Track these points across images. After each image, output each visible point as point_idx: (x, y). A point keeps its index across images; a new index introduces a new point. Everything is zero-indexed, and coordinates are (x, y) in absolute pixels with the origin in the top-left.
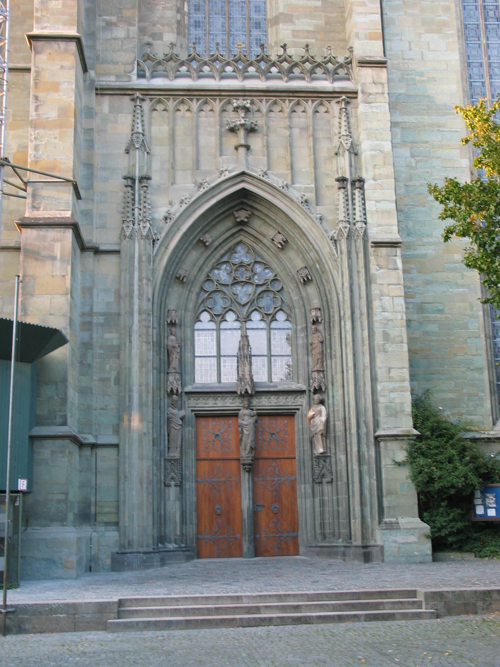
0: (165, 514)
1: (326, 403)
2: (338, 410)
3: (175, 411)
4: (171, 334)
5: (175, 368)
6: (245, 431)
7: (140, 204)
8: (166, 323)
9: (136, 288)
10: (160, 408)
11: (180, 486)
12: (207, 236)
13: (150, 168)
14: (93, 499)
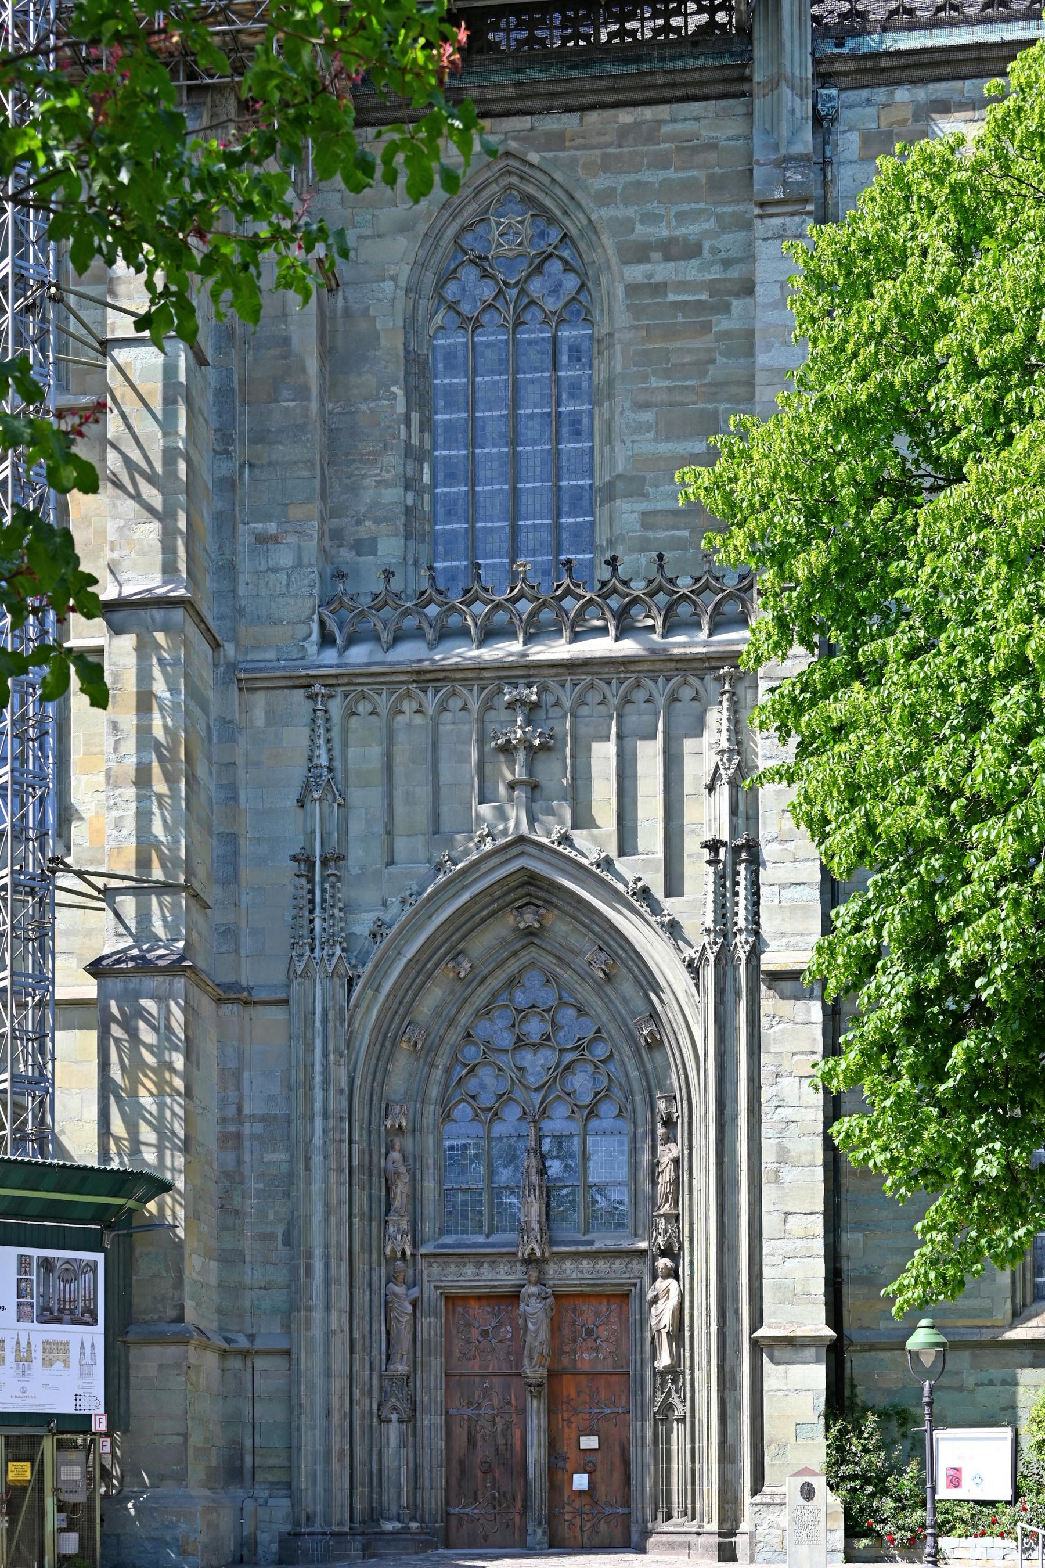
9: (318, 1068)
10: (370, 1285)
11: (411, 1419)
13: (346, 833)
14: (248, 1443)
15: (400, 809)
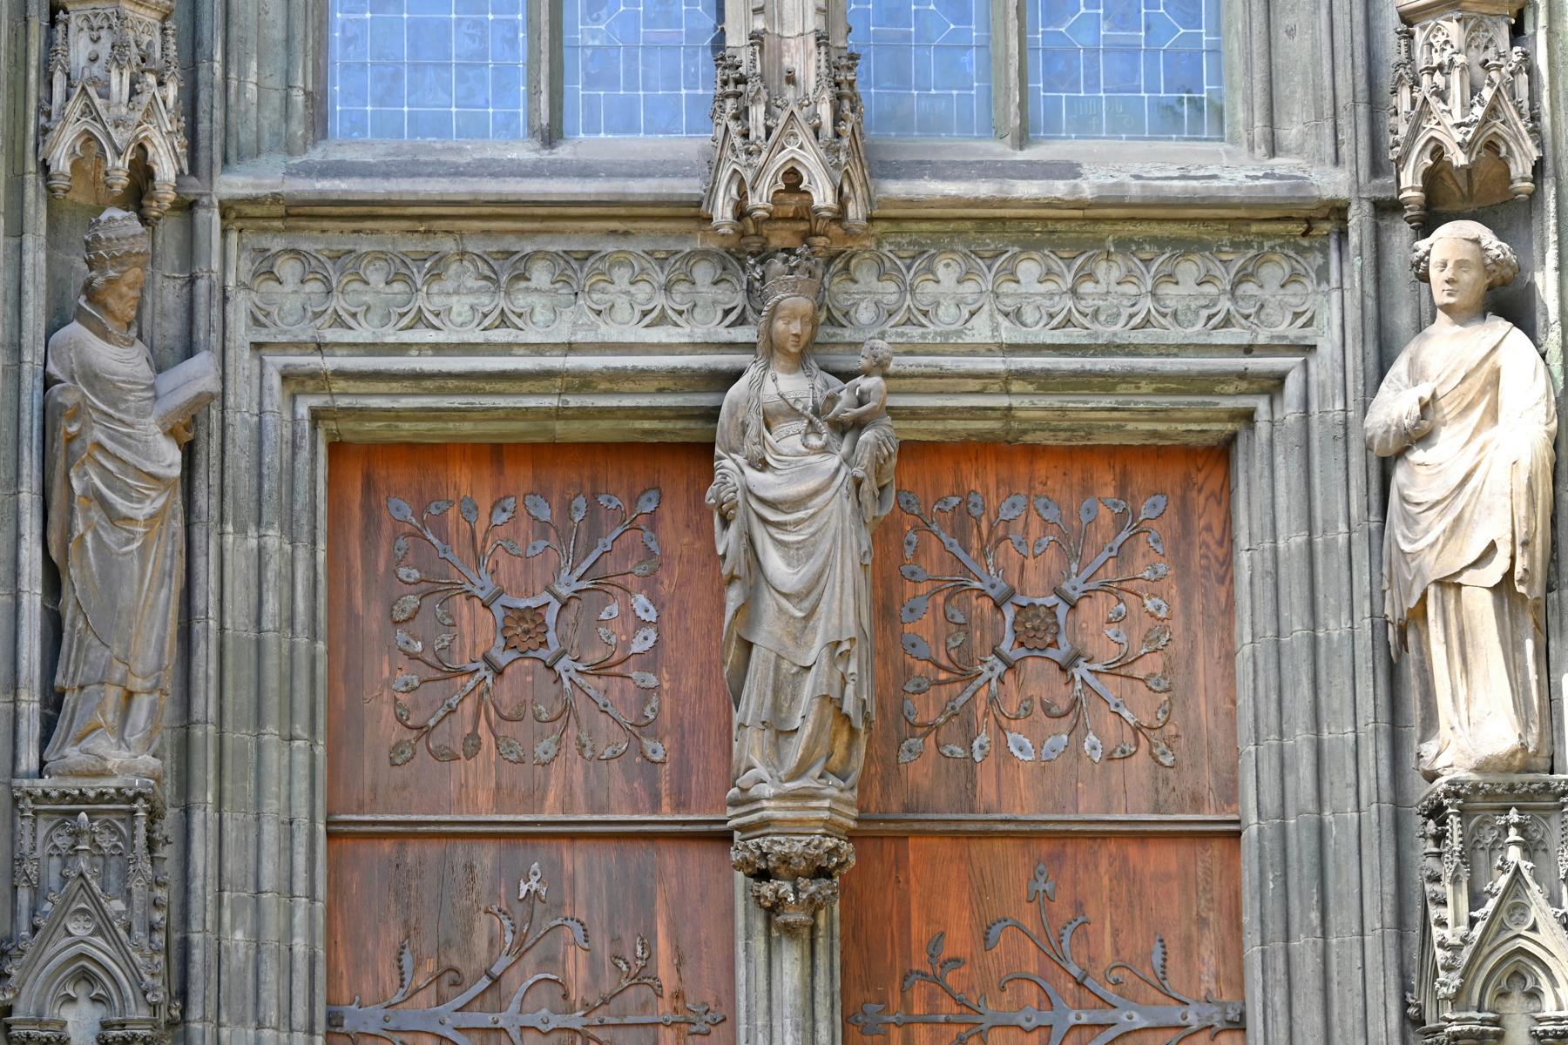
6: (774, 562)
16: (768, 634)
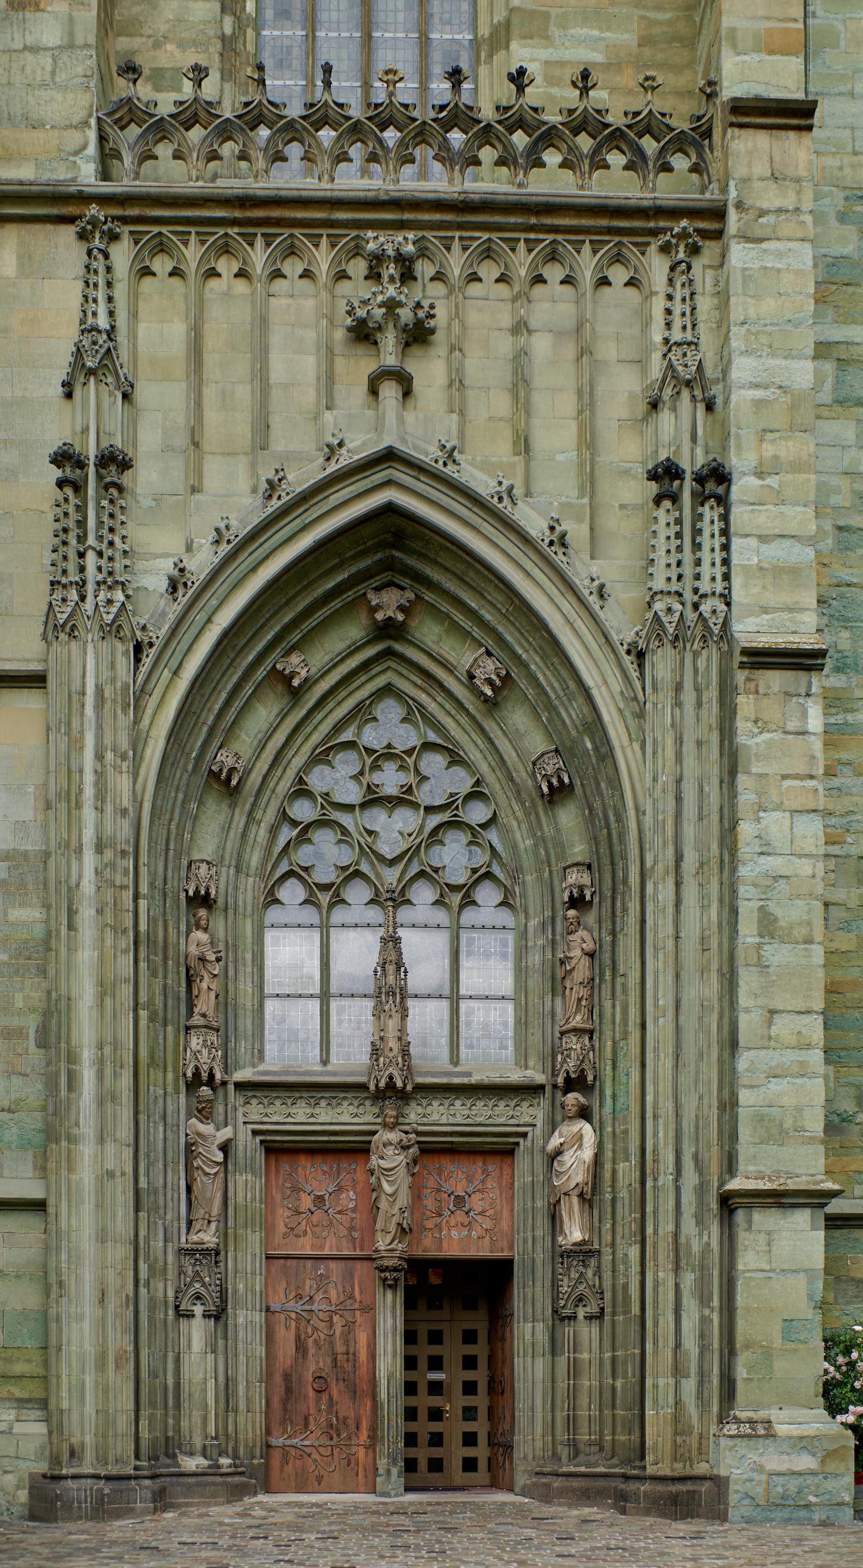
0: (177, 1385)
1: (596, 1118)
2: (626, 1132)
3: (206, 1129)
4: (198, 927)
5: (204, 1015)
6: (385, 1186)
7: (100, 538)
8: (183, 895)
12: (295, 659)
15: (212, 416)
16: (383, 1204)
